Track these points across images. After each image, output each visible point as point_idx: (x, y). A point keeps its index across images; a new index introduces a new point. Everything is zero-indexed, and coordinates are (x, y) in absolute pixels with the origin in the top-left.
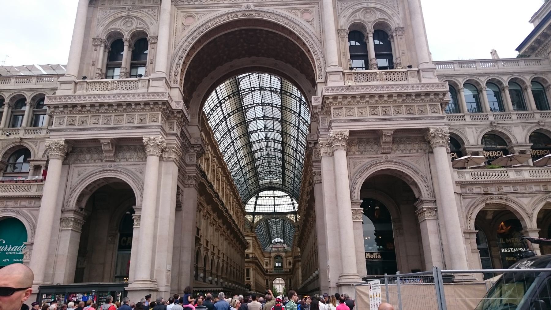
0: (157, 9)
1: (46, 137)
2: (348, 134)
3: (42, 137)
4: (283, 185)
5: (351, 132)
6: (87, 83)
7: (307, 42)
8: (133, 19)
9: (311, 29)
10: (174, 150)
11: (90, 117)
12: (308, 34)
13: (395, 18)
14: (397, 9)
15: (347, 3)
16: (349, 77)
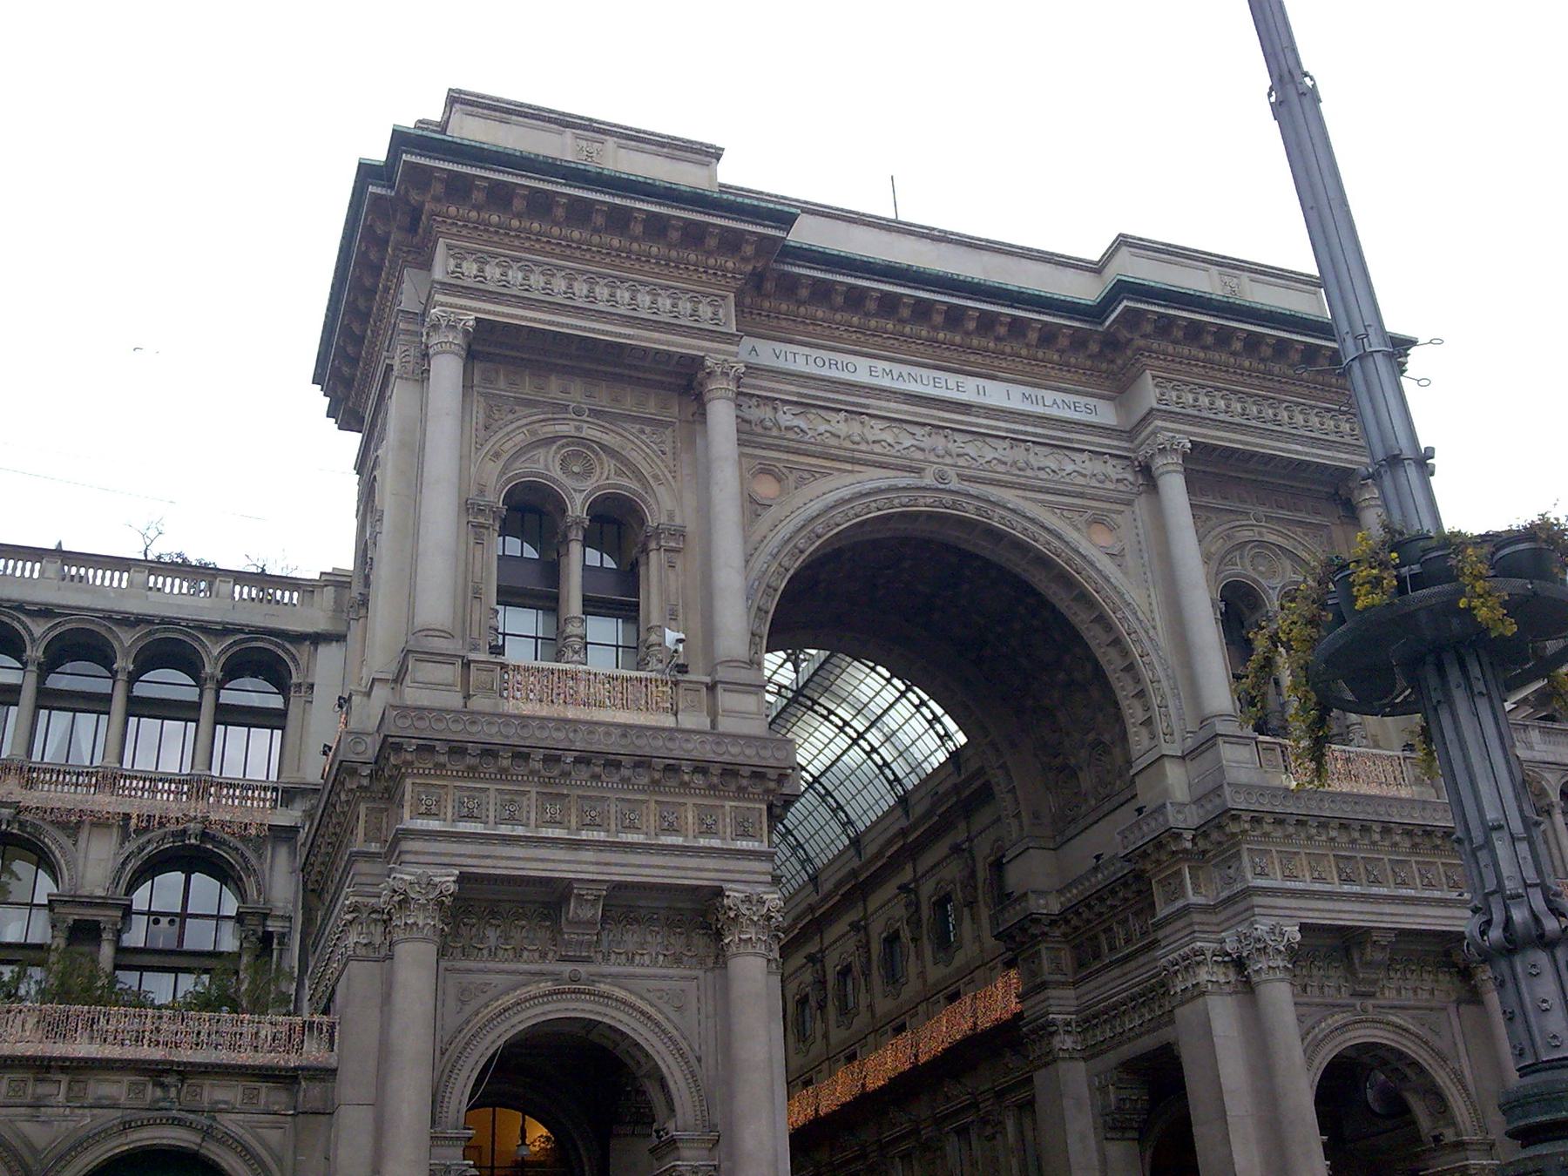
0: (669, 432)
2: (1298, 937)
5: (1303, 928)
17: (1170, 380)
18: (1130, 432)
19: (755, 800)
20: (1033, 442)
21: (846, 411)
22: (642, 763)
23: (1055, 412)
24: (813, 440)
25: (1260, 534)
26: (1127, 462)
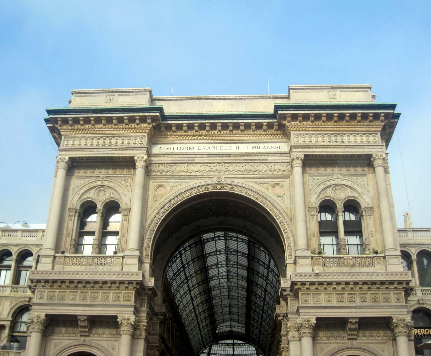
0: (130, 179)
1: (11, 295)
3: (7, 295)
5: (318, 319)
6: (65, 257)
8: (105, 188)
9: (281, 205)
11: (68, 292)
12: (279, 210)
13: (365, 197)
14: (367, 187)
15: (318, 179)
16: (318, 261)
18: (289, 153)
20: (253, 163)
24: (175, 174)
25: (338, 181)
26: (288, 164)
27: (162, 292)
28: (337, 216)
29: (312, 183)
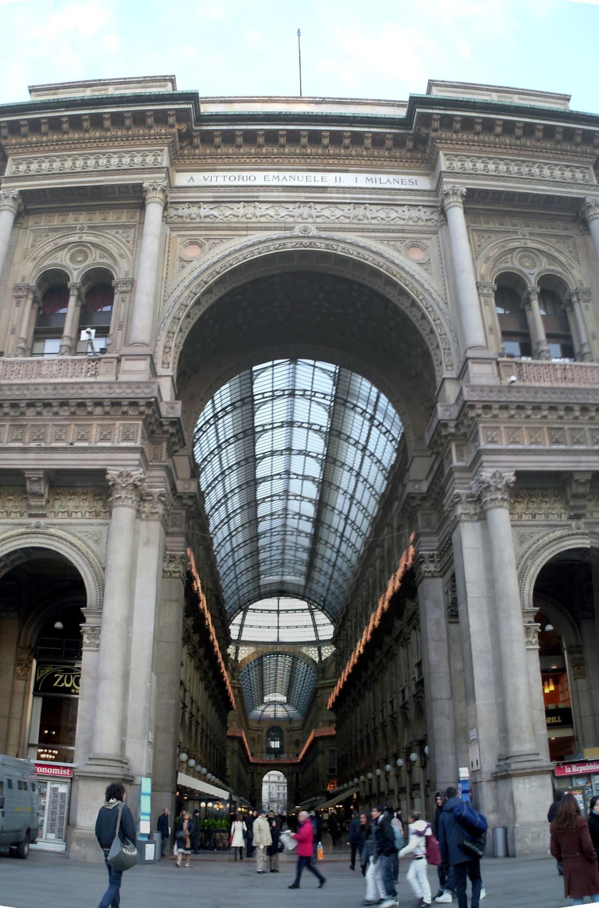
0: (132, 230)
2: (513, 479)
4: (305, 587)
5: (518, 474)
7: (421, 300)
8: (86, 246)
10: (163, 499)
15: (489, 237)
17: (456, 156)
18: (436, 191)
19: (135, 419)
20: (370, 204)
21: (244, 202)
22: (64, 403)
23: (388, 186)
25: (526, 243)
26: (435, 209)
27: (189, 459)
28: (529, 301)
29: (479, 243)
